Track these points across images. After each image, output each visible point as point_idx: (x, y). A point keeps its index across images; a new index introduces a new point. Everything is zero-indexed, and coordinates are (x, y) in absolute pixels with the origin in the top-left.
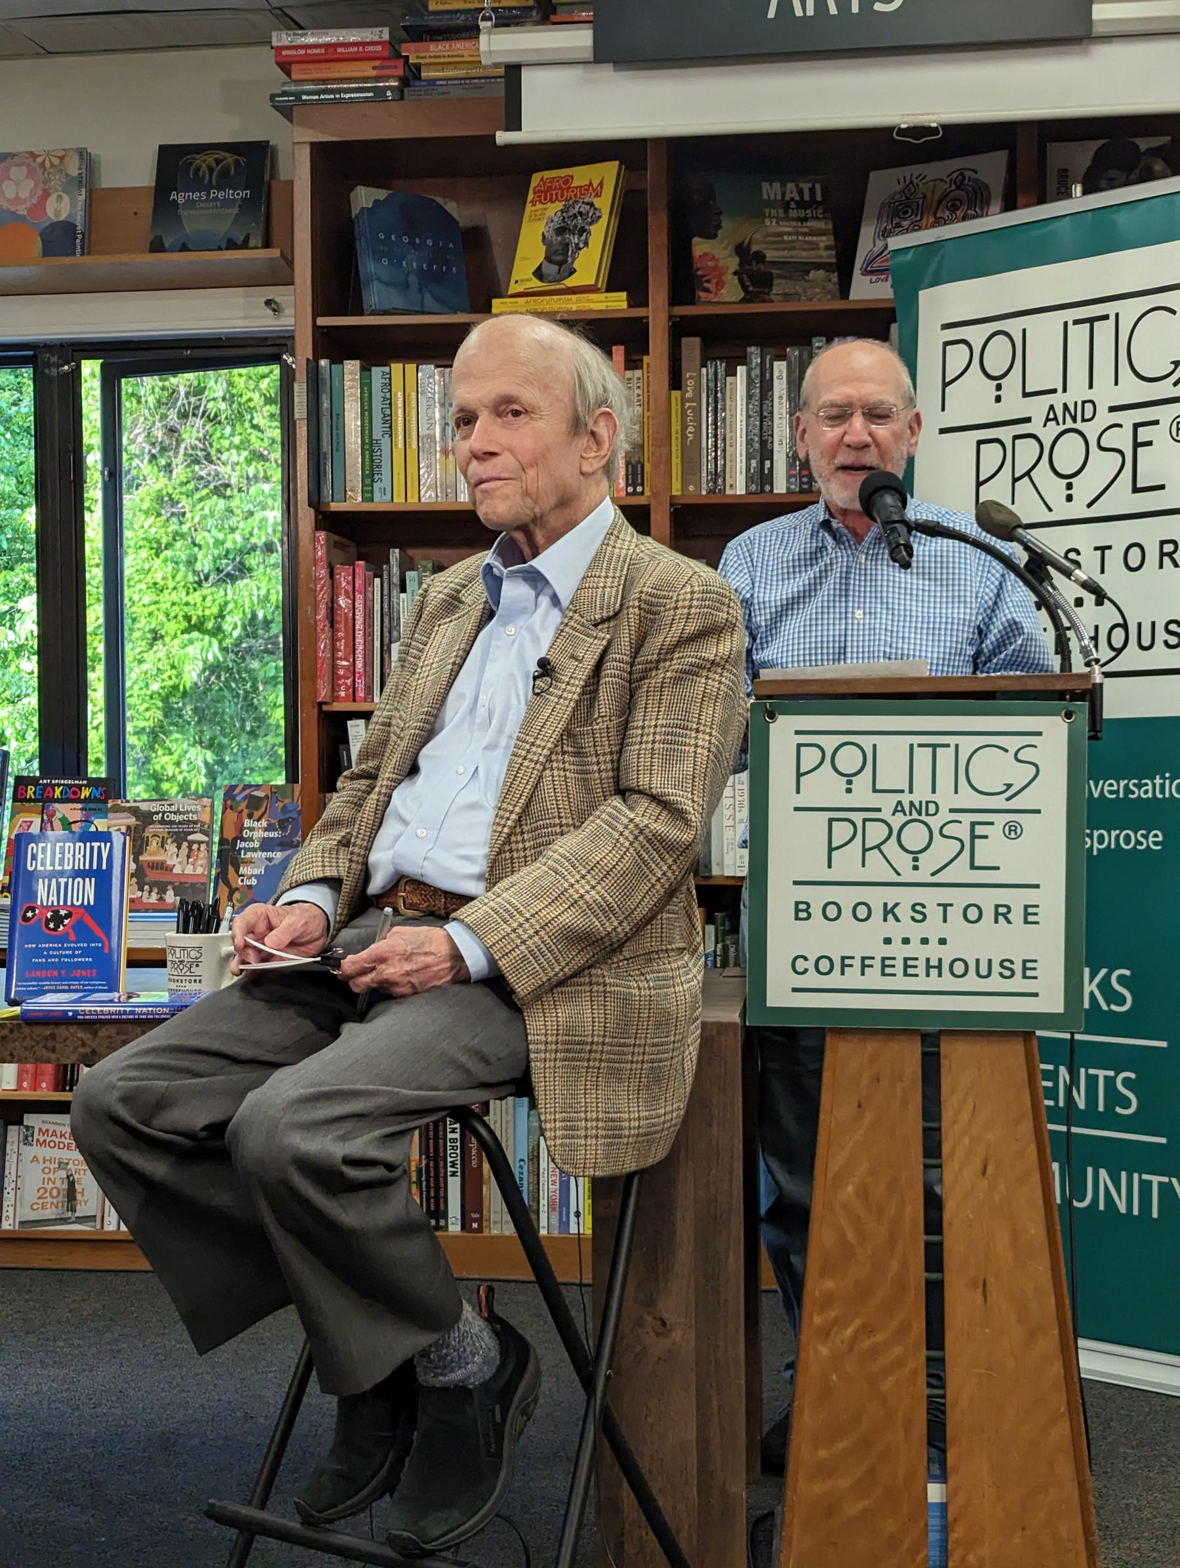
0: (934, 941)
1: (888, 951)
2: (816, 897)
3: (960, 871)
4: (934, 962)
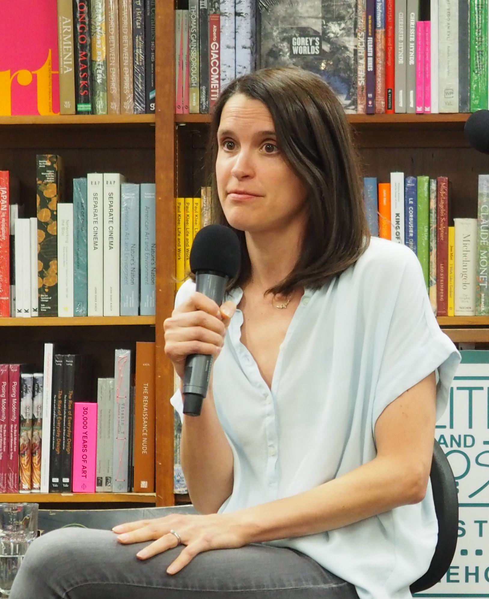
0: (472, 552)
4: (472, 570)
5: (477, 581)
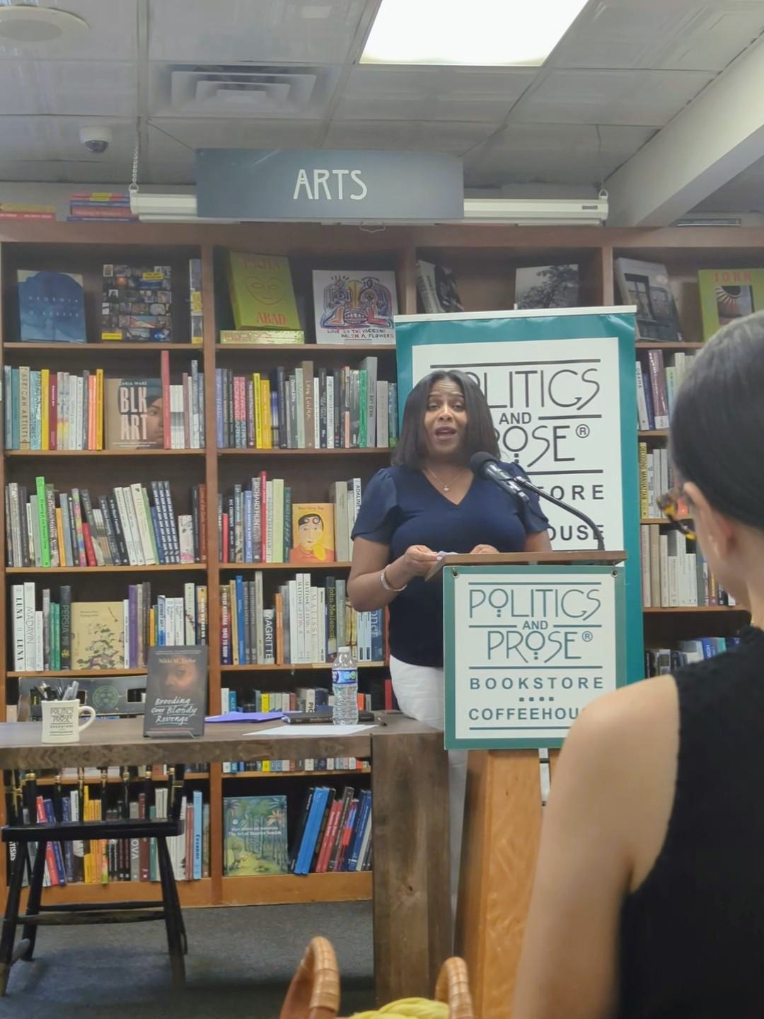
0: (547, 699)
1: (522, 705)
2: (483, 676)
3: (560, 660)
5: (550, 718)
